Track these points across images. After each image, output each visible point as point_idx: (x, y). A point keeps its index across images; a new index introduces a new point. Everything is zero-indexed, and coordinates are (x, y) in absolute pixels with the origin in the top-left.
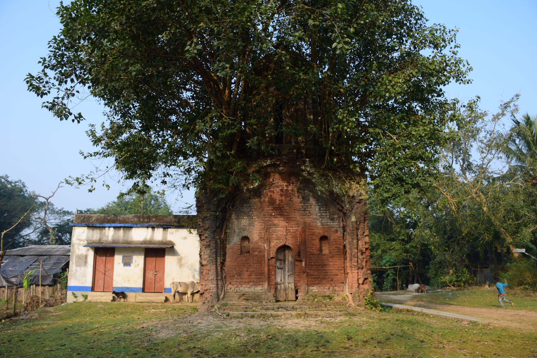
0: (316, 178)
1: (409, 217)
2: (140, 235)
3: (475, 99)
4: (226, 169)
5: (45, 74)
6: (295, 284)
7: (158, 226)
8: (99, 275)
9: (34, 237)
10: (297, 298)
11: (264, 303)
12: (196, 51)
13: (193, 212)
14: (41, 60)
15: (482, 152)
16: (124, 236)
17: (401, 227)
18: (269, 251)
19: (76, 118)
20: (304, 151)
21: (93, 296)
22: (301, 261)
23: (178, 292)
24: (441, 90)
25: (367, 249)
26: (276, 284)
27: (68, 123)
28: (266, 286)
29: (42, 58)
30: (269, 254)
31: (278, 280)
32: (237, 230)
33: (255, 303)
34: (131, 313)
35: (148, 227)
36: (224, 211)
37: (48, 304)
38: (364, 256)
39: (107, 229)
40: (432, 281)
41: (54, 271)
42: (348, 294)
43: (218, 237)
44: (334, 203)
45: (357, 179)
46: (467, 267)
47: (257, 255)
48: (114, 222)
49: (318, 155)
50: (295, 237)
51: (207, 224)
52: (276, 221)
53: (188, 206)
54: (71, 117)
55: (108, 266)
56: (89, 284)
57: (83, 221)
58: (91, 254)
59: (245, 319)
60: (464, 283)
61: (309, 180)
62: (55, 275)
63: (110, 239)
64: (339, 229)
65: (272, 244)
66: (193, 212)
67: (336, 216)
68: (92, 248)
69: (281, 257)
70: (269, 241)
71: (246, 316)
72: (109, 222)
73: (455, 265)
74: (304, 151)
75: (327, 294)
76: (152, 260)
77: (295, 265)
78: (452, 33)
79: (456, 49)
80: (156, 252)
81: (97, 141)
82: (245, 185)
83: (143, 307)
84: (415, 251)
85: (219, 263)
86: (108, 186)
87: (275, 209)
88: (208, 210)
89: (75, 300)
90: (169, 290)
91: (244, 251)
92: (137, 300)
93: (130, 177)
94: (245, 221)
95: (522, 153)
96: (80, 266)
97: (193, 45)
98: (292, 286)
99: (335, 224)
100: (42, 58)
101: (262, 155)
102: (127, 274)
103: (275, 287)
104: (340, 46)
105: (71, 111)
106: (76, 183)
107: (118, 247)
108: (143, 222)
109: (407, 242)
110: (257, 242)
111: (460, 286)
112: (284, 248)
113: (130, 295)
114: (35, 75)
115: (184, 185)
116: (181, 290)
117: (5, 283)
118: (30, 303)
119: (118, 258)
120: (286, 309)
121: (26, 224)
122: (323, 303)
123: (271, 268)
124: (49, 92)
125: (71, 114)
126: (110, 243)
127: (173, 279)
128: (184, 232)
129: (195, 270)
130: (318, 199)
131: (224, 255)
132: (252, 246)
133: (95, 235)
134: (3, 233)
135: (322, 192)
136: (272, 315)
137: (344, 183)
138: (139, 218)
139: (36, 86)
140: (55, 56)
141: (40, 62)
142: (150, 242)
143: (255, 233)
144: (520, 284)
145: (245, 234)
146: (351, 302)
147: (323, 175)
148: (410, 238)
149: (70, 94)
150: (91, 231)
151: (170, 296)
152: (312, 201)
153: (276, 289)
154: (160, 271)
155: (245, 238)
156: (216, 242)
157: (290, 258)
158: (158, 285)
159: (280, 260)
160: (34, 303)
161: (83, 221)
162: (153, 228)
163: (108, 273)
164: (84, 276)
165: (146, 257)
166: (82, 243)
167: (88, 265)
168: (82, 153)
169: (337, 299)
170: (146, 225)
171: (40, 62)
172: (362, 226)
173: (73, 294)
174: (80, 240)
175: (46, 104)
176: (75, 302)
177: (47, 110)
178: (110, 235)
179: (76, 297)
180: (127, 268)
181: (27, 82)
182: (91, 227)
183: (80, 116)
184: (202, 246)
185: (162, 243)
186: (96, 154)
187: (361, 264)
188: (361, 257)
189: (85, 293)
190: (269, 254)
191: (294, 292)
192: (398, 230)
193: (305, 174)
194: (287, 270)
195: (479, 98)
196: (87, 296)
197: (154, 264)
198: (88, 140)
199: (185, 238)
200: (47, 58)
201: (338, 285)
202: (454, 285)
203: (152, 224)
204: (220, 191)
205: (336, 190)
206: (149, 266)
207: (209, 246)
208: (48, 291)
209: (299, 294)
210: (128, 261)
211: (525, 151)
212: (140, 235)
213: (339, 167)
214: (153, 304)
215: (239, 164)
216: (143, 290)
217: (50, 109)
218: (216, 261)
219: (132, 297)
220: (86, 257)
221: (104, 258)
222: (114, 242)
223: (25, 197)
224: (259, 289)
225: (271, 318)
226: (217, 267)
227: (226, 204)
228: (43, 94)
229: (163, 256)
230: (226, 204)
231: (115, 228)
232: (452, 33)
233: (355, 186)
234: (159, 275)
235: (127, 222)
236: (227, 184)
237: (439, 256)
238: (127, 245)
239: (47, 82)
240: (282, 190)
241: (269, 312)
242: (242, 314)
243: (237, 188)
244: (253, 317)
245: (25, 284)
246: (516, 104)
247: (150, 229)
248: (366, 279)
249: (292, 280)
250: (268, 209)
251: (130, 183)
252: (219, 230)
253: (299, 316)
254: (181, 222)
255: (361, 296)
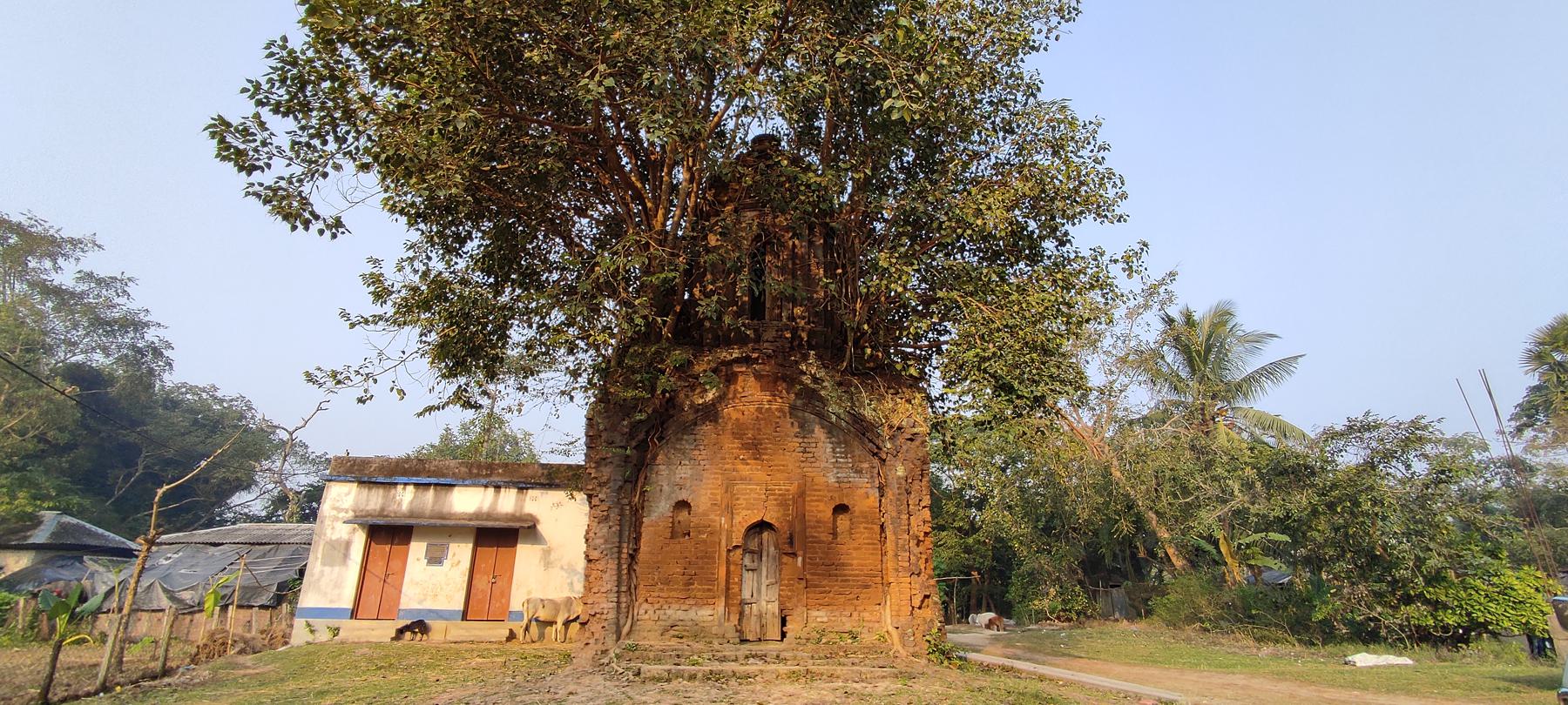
0: (828, 390)
1: (971, 487)
2: (468, 501)
3: (1137, 248)
4: (650, 365)
5: (262, 125)
6: (781, 603)
7: (508, 485)
8: (373, 583)
9: (259, 507)
10: (784, 635)
11: (716, 645)
12: (602, 90)
13: (578, 458)
14: (249, 86)
15: (1112, 373)
16: (435, 502)
17: (958, 505)
18: (729, 533)
19: (328, 226)
20: (804, 335)
21: (353, 630)
22: (794, 555)
23: (537, 620)
24: (1066, 234)
25: (926, 534)
26: (743, 603)
27: (309, 239)
28: (721, 607)
29: (250, 81)
30: (729, 539)
31: (746, 595)
32: (666, 488)
33: (696, 646)
34: (428, 666)
35: (486, 486)
36: (642, 447)
37: (248, 648)
38: (921, 549)
39: (400, 487)
40: (1018, 608)
41: (282, 578)
42: (890, 628)
43: (626, 501)
44: (860, 433)
45: (908, 393)
46: (1080, 582)
47: (704, 541)
48: (416, 473)
49: (831, 339)
50: (783, 504)
51: (606, 472)
52: (745, 470)
53: (570, 439)
54: (316, 226)
55: (395, 564)
56: (347, 602)
57: (349, 471)
58: (360, 539)
59: (674, 683)
60: (1078, 614)
61: (814, 390)
62: (281, 586)
63: (405, 507)
64: (871, 492)
65: (737, 519)
66: (578, 458)
67: (866, 465)
68: (362, 525)
69: (753, 545)
70: (730, 510)
71: (679, 675)
72: (405, 473)
73: (1058, 578)
74: (804, 335)
75: (848, 627)
76: (488, 553)
77: (781, 563)
78: (1091, 128)
79: (1102, 153)
80: (498, 537)
81: (381, 295)
82: (687, 396)
83: (458, 653)
84: (983, 549)
85: (624, 556)
86: (402, 393)
87: (745, 447)
88: (610, 443)
89: (310, 638)
90: (520, 615)
91: (677, 532)
92: (449, 638)
93: (451, 374)
94: (684, 472)
95: (1180, 380)
96: (332, 565)
97: (597, 78)
98: (774, 608)
99: (863, 481)
100: (250, 81)
101: (724, 341)
102: (433, 581)
103: (739, 608)
104: (899, 104)
105: (318, 212)
106: (331, 383)
107: (420, 526)
108: (478, 475)
109: (967, 534)
110: (705, 514)
111: (1069, 620)
112: (761, 526)
113: (436, 625)
114: (235, 120)
115: (563, 393)
116: (543, 615)
117: (165, 602)
118: (205, 645)
119: (418, 549)
120: (763, 657)
121: (246, 484)
122: (840, 648)
123: (732, 568)
124: (269, 166)
125: (317, 217)
126: (405, 517)
127: (529, 593)
128: (559, 495)
129: (574, 571)
130: (831, 429)
131: (637, 539)
132: (695, 520)
133: (374, 500)
134: (160, 492)
135: (838, 416)
136: (734, 674)
137: (881, 398)
138: (470, 466)
139: (235, 146)
140: (283, 81)
141: (245, 90)
142: (489, 516)
143: (704, 496)
144: (1193, 618)
145: (683, 496)
146: (898, 646)
147: (840, 384)
148: (974, 528)
149: (315, 170)
150: (365, 491)
151: (519, 628)
152: (819, 433)
153: (741, 614)
154: (504, 575)
155: (683, 505)
156: (622, 509)
157: (772, 549)
158: (496, 605)
159: (752, 552)
160: (217, 646)
161: (349, 471)
162: (497, 487)
163: (393, 578)
164: (338, 585)
165: (476, 545)
166: (342, 515)
167: (350, 563)
168: (345, 315)
169: (867, 638)
170: (484, 481)
171: (245, 90)
172: (916, 485)
173: (309, 625)
174: (339, 510)
175: (257, 188)
176: (309, 643)
177: (257, 203)
178: (405, 499)
179: (312, 632)
180: (435, 568)
181: (213, 135)
182: (366, 482)
183: (338, 223)
184: (592, 517)
185: (513, 517)
186: (377, 319)
187: (916, 565)
188: (916, 550)
189: (335, 623)
190: (729, 539)
191: (778, 622)
192: (953, 510)
193: (806, 380)
194: (764, 573)
195: (1146, 245)
196: (338, 629)
197: (491, 561)
198: (365, 293)
199: (559, 505)
200: (263, 81)
201: (870, 608)
202: (1058, 618)
203: (495, 479)
204: (636, 405)
205: (868, 413)
206: (482, 565)
207: (607, 518)
208: (260, 619)
209: (789, 626)
210: (437, 555)
211: (1183, 375)
212: (468, 501)
213: (872, 369)
214: (483, 646)
215: (678, 355)
216: (464, 617)
217: (267, 201)
218: (620, 552)
219: (439, 631)
220: (348, 544)
221: (387, 547)
222: (411, 515)
223: (247, 430)
224: (704, 614)
225: (733, 682)
226: (619, 565)
227: (647, 433)
228: (250, 170)
229: (514, 545)
230: (647, 433)
231: (417, 485)
232: (1091, 128)
233: (902, 406)
234: (499, 583)
235: (444, 476)
236: (653, 390)
237: (1030, 559)
238: (439, 522)
239: (264, 144)
240: (759, 410)
241: (729, 667)
242: (669, 671)
243: (671, 403)
244: (692, 677)
245: (209, 604)
246: (1169, 288)
247: (491, 490)
248: (927, 597)
249: (773, 594)
250: (731, 445)
251: (451, 388)
252: (629, 486)
253: (793, 676)
254: (553, 478)
255: (919, 635)
